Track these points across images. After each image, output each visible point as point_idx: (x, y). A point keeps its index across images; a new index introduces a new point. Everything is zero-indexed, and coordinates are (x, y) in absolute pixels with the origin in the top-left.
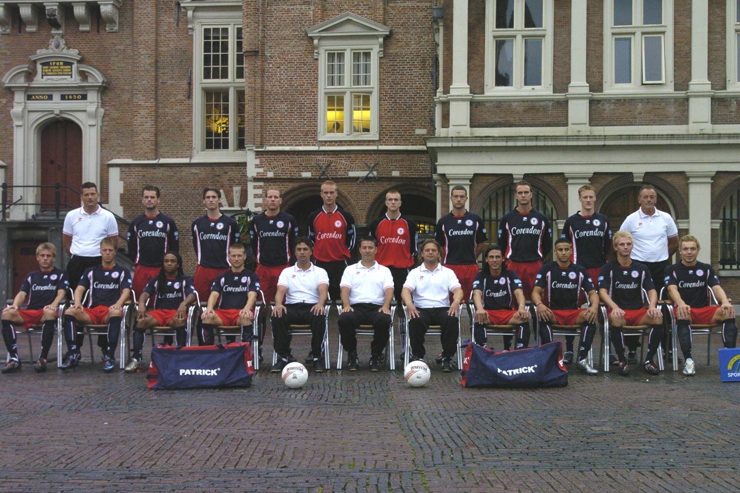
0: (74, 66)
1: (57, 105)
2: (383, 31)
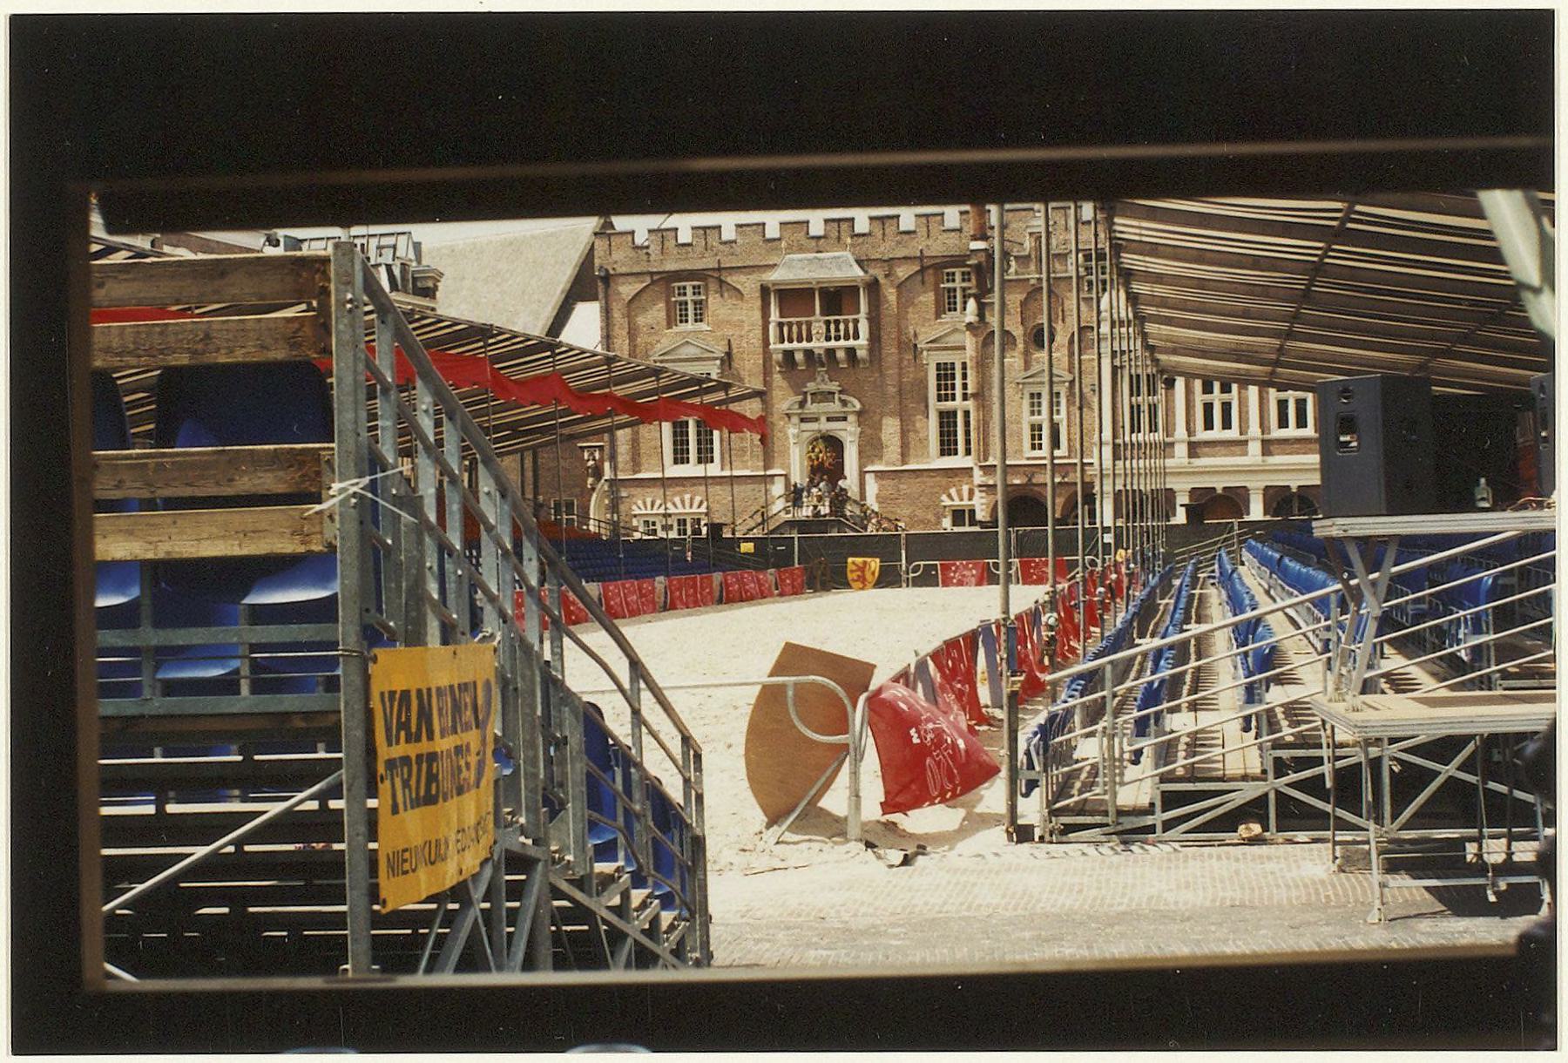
0: (836, 396)
1: (824, 426)
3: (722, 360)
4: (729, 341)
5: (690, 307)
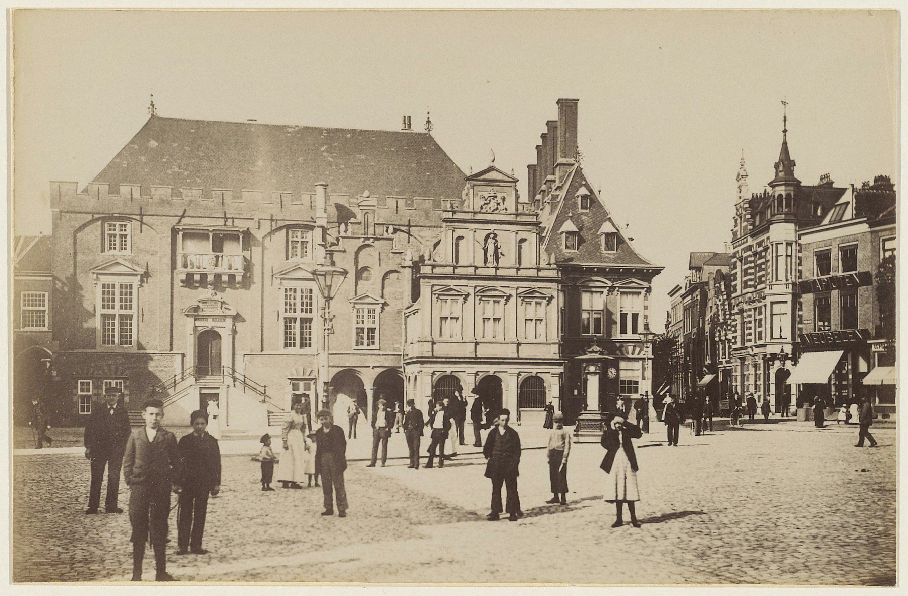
1: (209, 324)
2: (383, 301)
3: (142, 275)
4: (147, 263)
5: (117, 238)
